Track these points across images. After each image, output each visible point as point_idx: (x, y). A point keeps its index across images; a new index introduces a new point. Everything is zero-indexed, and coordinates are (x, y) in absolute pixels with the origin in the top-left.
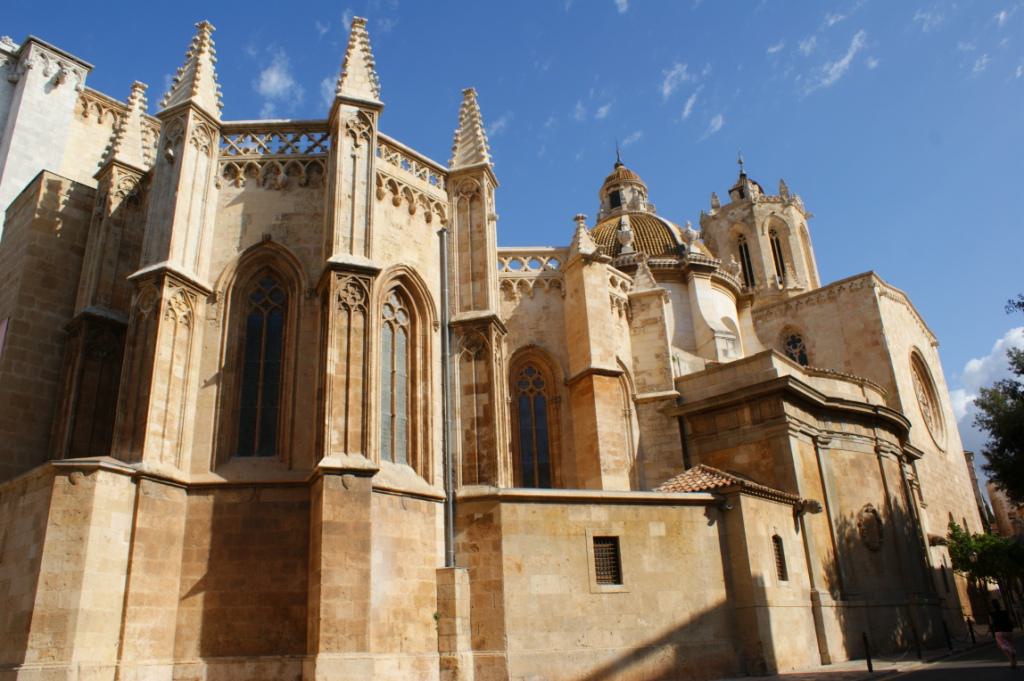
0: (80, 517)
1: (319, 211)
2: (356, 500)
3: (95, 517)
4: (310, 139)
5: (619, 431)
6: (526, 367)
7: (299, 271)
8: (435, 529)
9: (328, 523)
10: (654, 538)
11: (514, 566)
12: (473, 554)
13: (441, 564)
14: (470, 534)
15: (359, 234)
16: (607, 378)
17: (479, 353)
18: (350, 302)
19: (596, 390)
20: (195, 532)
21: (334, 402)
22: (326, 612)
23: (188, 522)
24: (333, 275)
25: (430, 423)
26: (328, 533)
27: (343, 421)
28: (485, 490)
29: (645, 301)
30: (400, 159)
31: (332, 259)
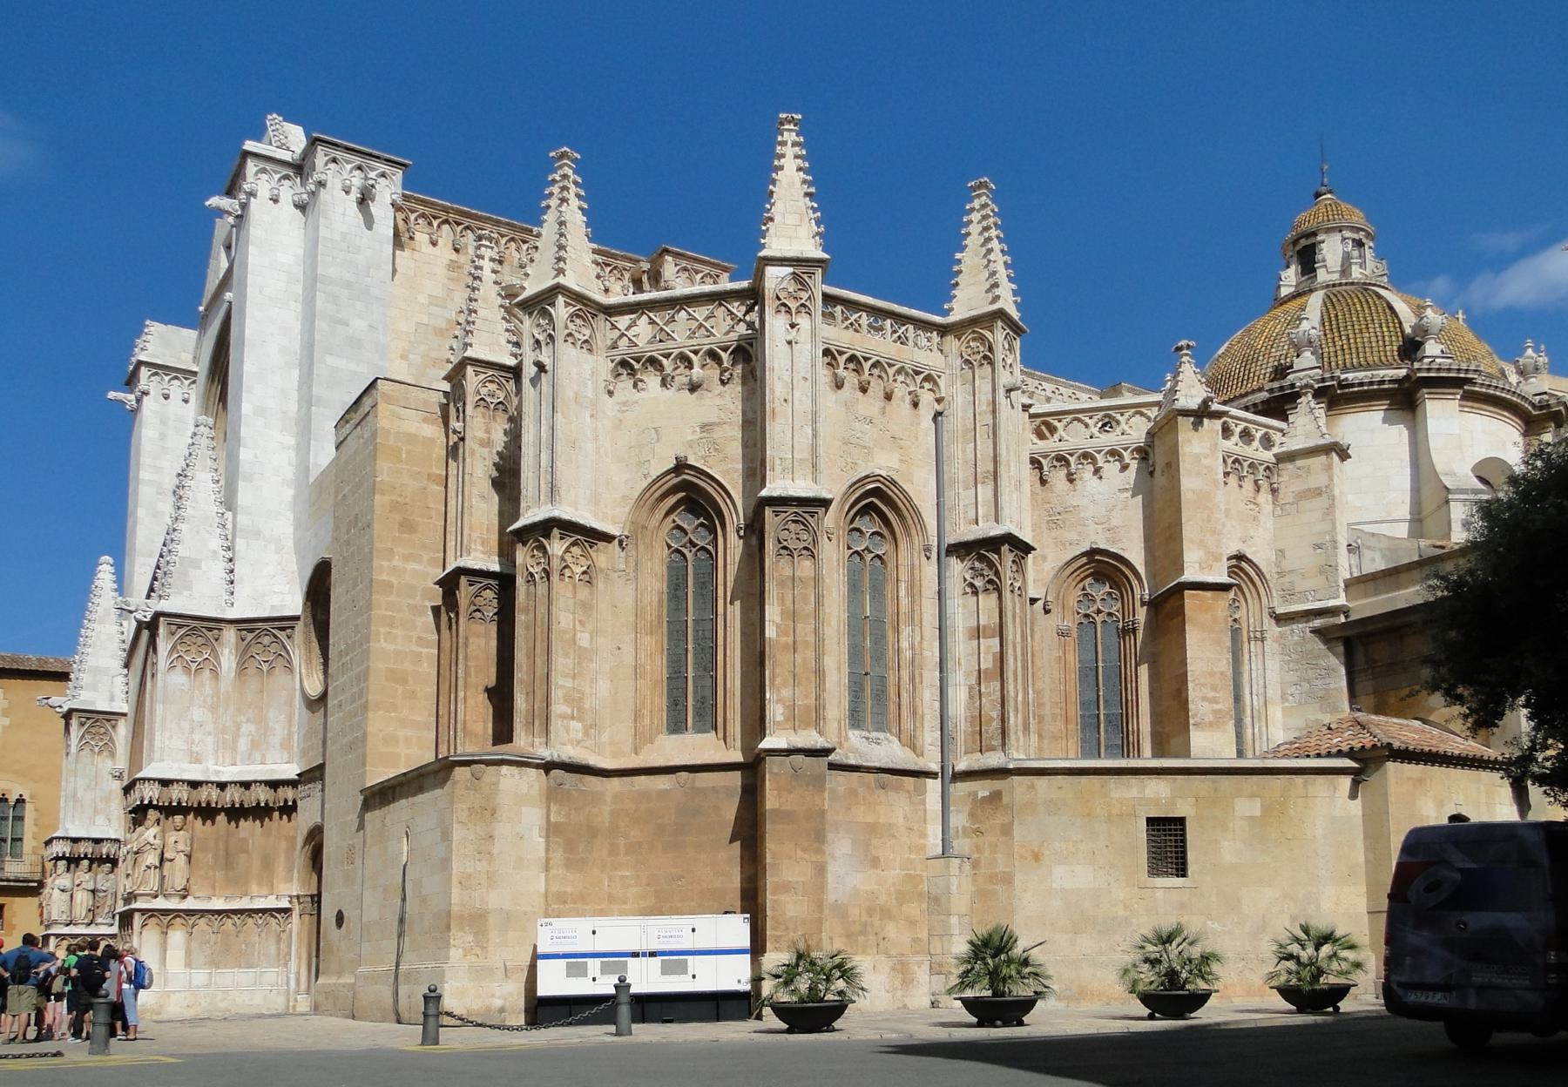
0: (487, 814)
9: (773, 811)
15: (803, 453)
16: (1209, 594)
21: (778, 671)
22: (773, 908)
24: (768, 511)
25: (917, 680)
27: (791, 693)
30: (865, 319)
31: (764, 493)
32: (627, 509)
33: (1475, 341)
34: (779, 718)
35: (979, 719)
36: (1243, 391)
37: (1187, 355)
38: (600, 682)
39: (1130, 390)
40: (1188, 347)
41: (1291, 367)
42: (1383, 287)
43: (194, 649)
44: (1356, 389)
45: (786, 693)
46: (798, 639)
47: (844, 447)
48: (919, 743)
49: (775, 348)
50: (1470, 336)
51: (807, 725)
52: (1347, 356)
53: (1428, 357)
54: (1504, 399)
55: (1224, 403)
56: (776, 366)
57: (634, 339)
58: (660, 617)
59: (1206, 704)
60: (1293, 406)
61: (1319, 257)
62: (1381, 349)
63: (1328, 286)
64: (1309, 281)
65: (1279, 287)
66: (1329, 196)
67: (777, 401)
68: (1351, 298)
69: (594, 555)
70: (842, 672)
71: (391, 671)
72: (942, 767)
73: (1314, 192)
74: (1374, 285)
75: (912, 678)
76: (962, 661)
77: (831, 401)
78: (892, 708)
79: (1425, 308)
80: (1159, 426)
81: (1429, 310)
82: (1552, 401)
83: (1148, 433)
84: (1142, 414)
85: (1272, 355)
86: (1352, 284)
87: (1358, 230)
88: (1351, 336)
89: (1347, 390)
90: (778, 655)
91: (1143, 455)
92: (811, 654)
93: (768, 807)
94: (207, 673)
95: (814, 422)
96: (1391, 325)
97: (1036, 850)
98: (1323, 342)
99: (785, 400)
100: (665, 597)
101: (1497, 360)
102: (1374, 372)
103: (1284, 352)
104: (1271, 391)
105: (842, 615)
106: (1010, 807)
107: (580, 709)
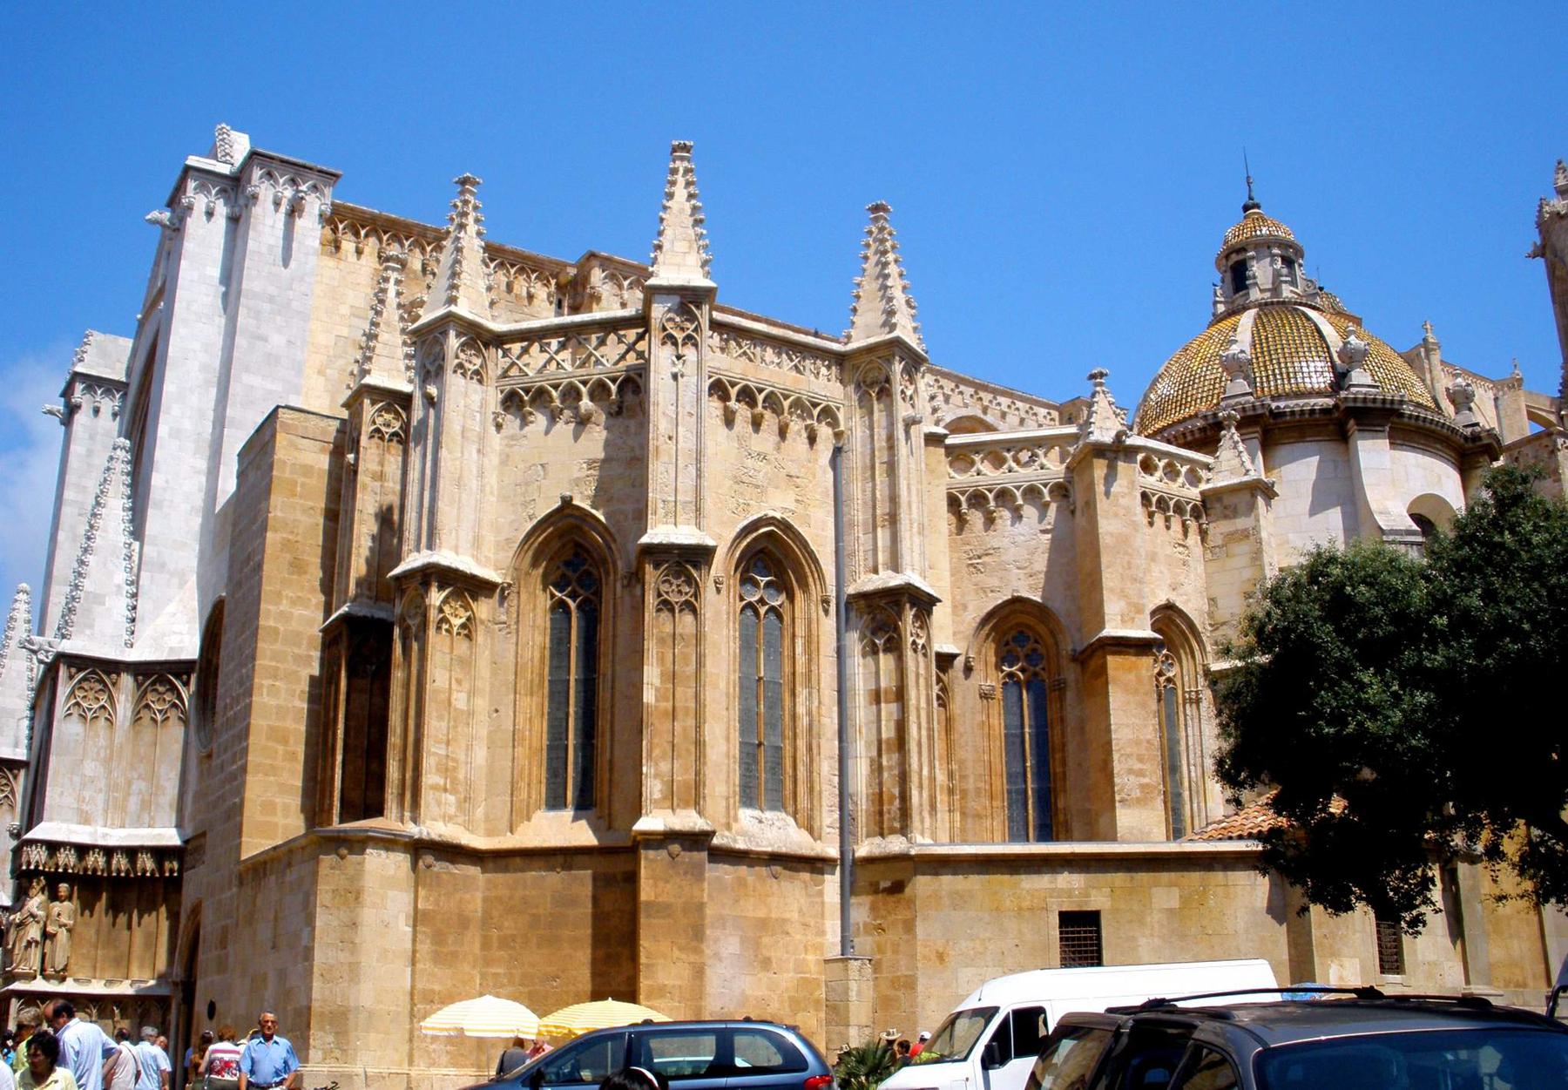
1: (638, 452)
2: (686, 873)
3: (367, 898)
4: (620, 341)
5: (1149, 737)
6: (1014, 633)
7: (613, 546)
8: (823, 903)
9: (648, 903)
10: (1160, 911)
11: (933, 957)
12: (877, 938)
13: (836, 952)
14: (874, 908)
15: (686, 495)
17: (889, 640)
18: (673, 598)
19: (1110, 672)
20: (495, 914)
21: (656, 741)
23: (485, 900)
25: (815, 751)
26: (649, 916)
27: (670, 766)
28: (896, 845)
29: (1227, 500)
32: (511, 554)
34: (657, 795)
35: (879, 798)
38: (476, 748)
43: (91, 695)
45: (665, 767)
46: (677, 704)
47: (736, 487)
48: (816, 825)
49: (661, 382)
51: (686, 805)
56: (661, 401)
57: (525, 369)
58: (541, 676)
59: (1132, 778)
67: (661, 439)
69: (474, 606)
70: (732, 742)
71: (271, 728)
72: (842, 853)
75: (810, 749)
76: (864, 731)
77: (718, 439)
78: (789, 784)
90: (656, 722)
92: (691, 722)
93: (643, 897)
94: (102, 722)
95: (698, 461)
97: (941, 950)
99: (670, 438)
100: (547, 653)
105: (732, 677)
106: (911, 902)
107: (454, 780)
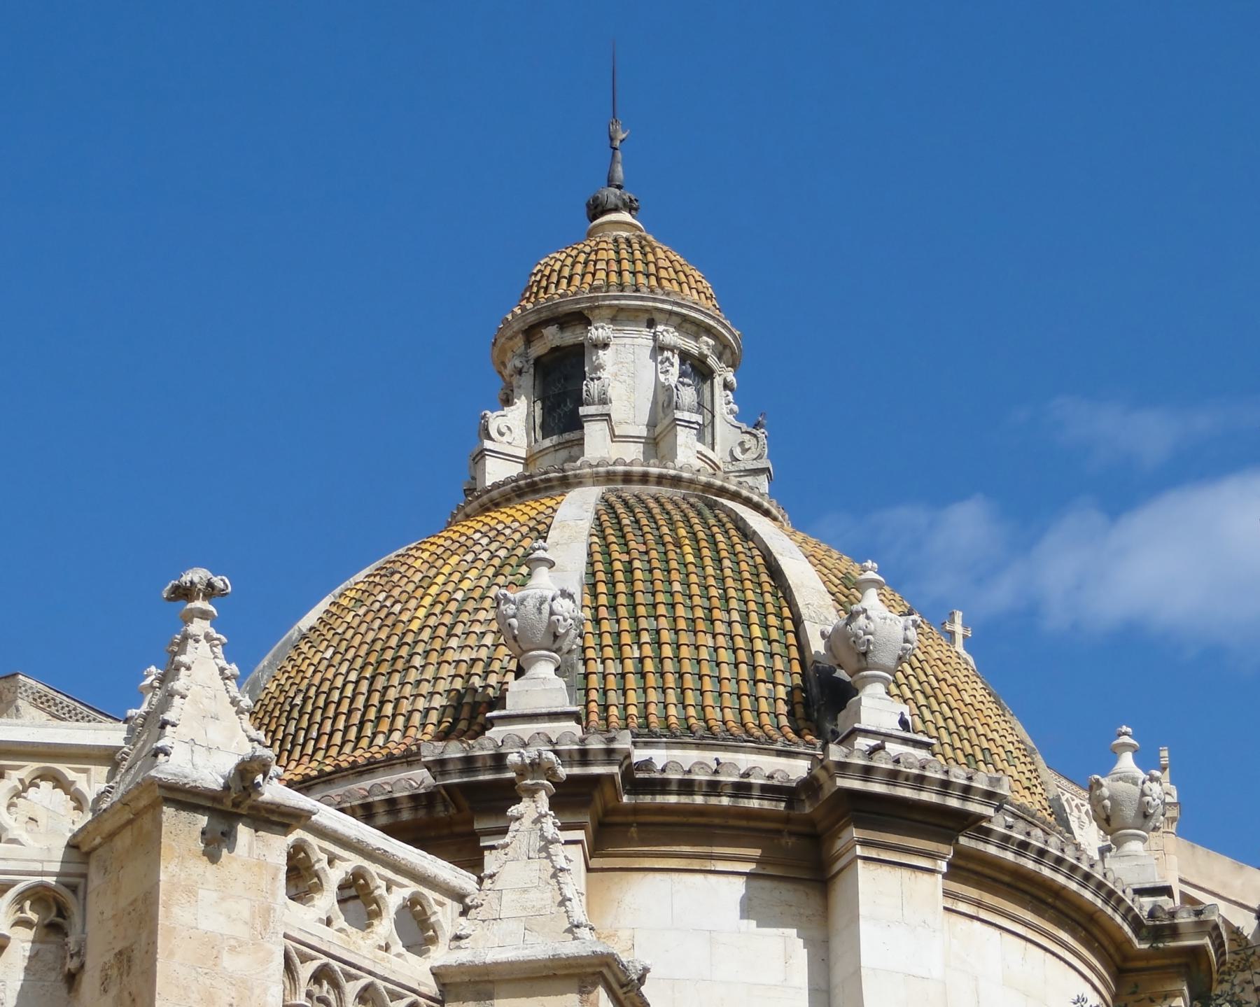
33: (990, 708)
36: (361, 756)
37: (204, 615)
39: (40, 702)
40: (210, 591)
41: (499, 702)
42: (757, 507)
44: (673, 799)
50: (976, 691)
52: (653, 696)
53: (866, 733)
54: (1058, 893)
55: (304, 785)
60: (501, 823)
61: (591, 388)
62: (745, 688)
63: (610, 477)
64: (563, 454)
65: (481, 454)
66: (625, 216)
68: (671, 522)
73: (588, 196)
74: (735, 496)
79: (862, 586)
80: (108, 826)
81: (872, 593)
82: (1184, 918)
83: (72, 846)
84: (59, 782)
85: (450, 656)
86: (676, 481)
87: (698, 329)
88: (666, 636)
89: (647, 799)
91: (52, 917)
96: (772, 620)
98: (591, 641)
101: (1047, 775)
102: (725, 757)
103: (483, 654)
104: (439, 766)
